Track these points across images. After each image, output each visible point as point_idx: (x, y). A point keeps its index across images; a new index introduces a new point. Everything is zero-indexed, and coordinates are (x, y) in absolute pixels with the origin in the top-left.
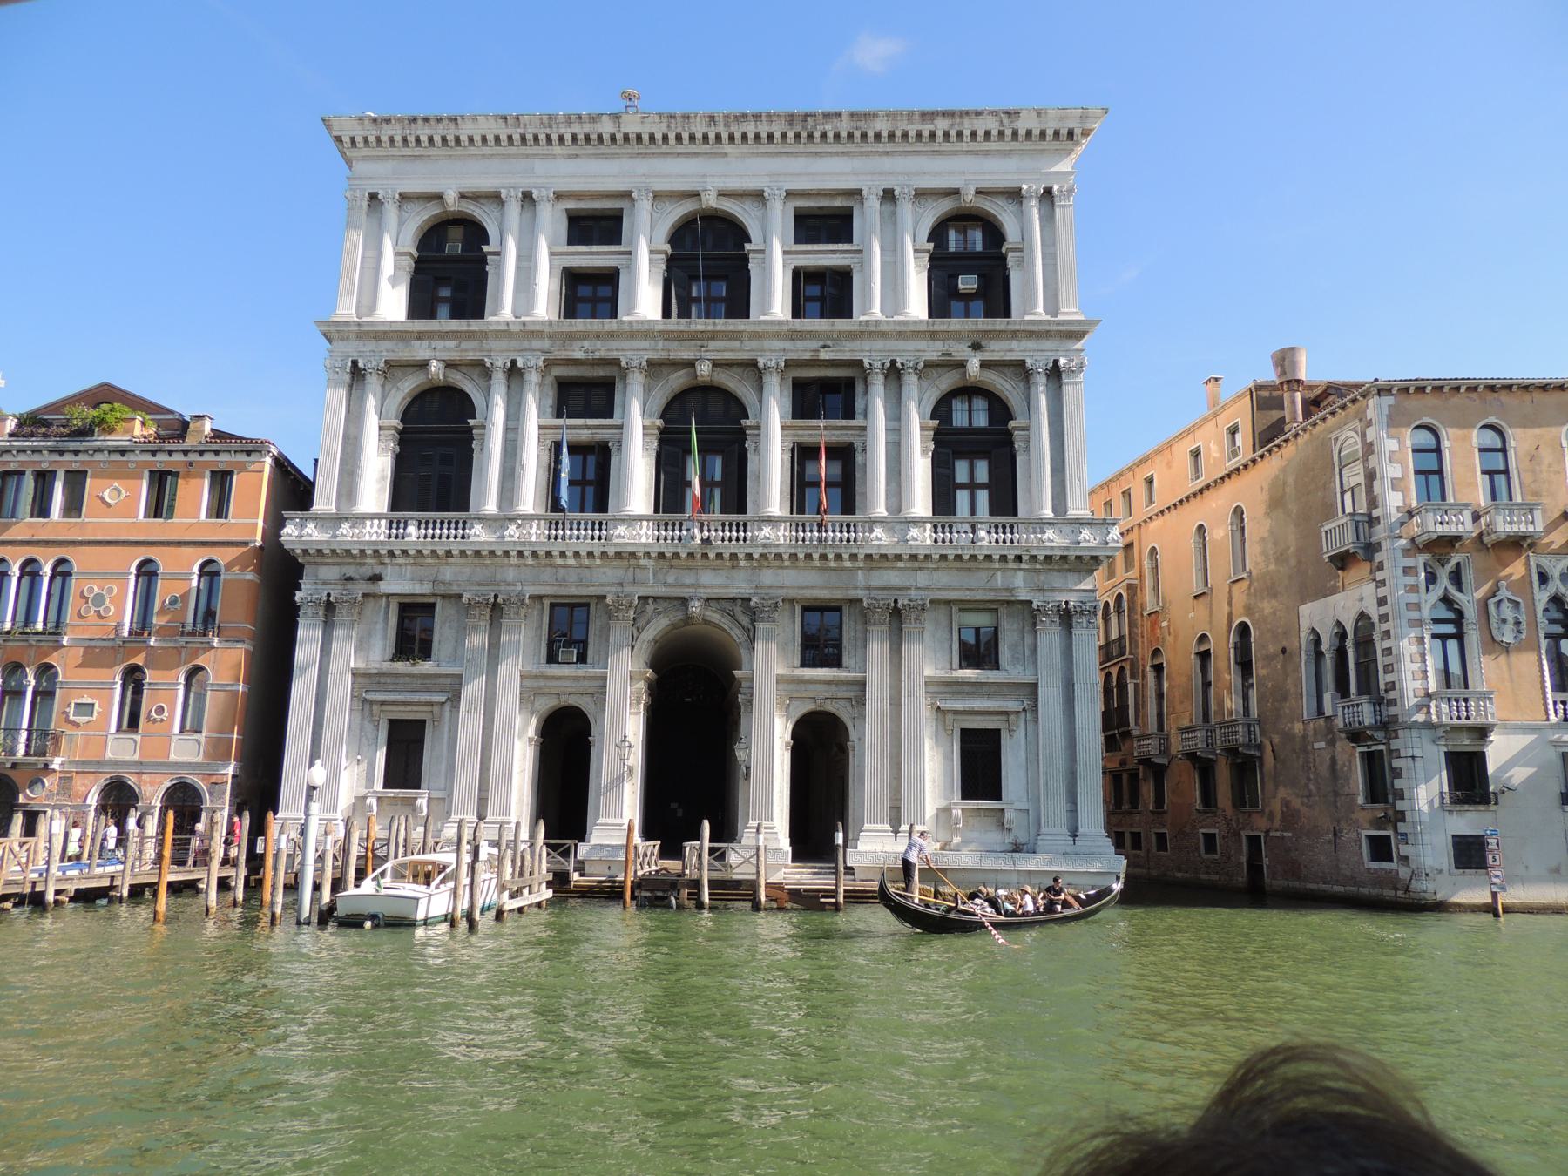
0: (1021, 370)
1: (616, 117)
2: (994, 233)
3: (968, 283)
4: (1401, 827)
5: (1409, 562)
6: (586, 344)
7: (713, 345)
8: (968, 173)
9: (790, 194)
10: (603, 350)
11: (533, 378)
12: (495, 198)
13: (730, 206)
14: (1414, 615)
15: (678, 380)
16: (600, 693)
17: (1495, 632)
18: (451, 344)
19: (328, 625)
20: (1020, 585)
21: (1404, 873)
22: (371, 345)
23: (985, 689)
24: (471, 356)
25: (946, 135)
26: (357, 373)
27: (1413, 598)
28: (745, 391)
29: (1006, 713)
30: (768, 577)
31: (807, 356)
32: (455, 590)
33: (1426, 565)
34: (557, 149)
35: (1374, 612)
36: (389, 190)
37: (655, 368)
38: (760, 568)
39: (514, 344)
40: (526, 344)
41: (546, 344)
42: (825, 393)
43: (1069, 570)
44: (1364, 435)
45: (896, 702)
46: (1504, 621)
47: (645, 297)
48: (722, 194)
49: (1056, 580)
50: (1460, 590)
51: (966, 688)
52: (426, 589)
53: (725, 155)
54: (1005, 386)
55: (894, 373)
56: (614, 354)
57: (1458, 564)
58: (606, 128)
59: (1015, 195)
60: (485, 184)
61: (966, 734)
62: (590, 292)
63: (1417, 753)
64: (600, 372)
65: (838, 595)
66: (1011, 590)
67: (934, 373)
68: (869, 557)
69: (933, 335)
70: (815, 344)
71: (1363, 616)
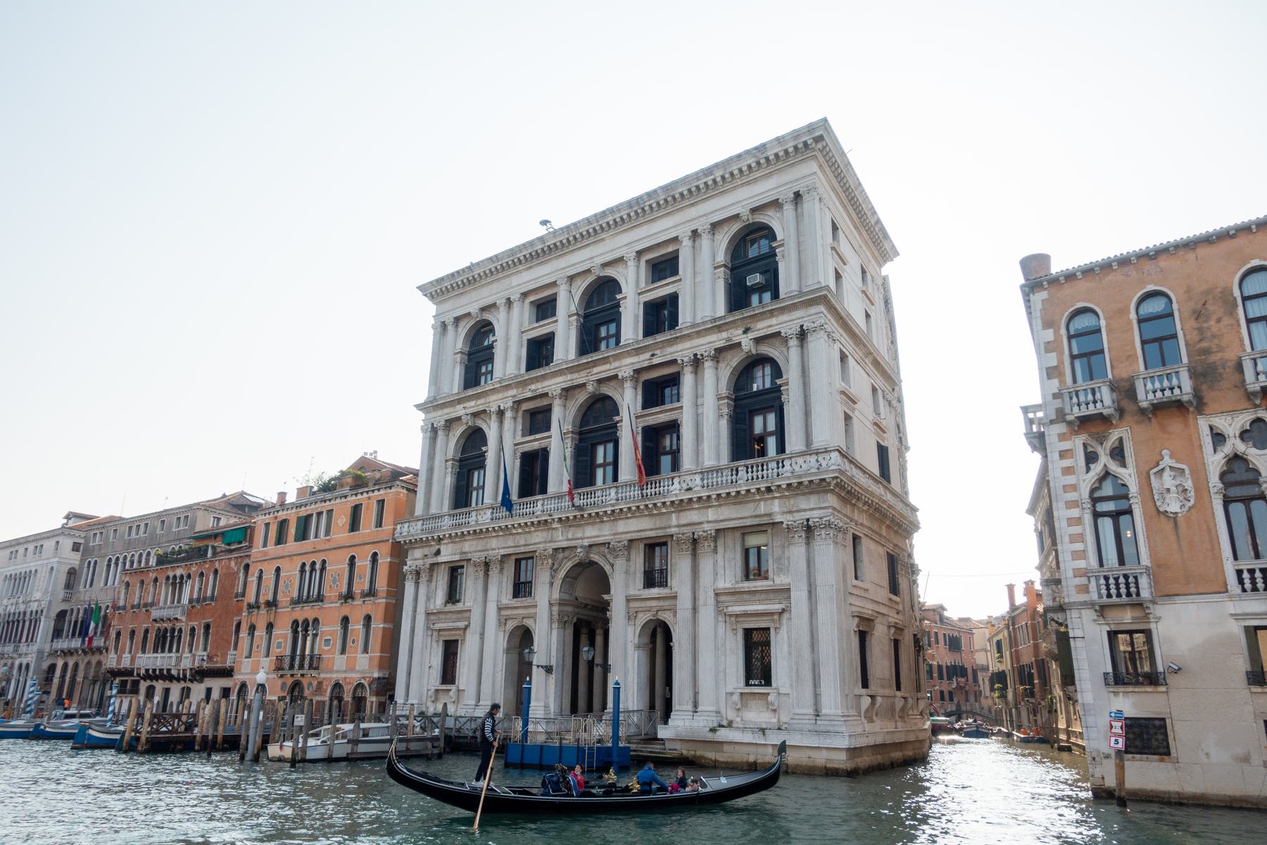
1: (541, 239)
2: (771, 235)
3: (755, 279)
5: (1066, 445)
6: (533, 387)
7: (596, 370)
10: (539, 387)
11: (509, 414)
12: (493, 306)
13: (610, 272)
14: (1072, 496)
15: (582, 397)
16: (533, 617)
17: (1158, 504)
18: (472, 403)
19: (417, 584)
20: (776, 508)
22: (440, 413)
23: (758, 596)
24: (481, 408)
25: (723, 178)
27: (1070, 480)
29: (772, 614)
30: (622, 526)
31: (646, 364)
32: (469, 556)
33: (1085, 446)
34: (521, 268)
37: (567, 392)
38: (616, 520)
39: (500, 396)
40: (506, 394)
41: (513, 392)
42: (659, 388)
43: (810, 493)
45: (695, 609)
46: (1168, 490)
47: (565, 347)
48: (605, 265)
49: (803, 502)
50: (1124, 465)
51: (746, 596)
52: (457, 558)
53: (603, 240)
55: (697, 362)
56: (546, 390)
57: (1121, 440)
58: (539, 247)
59: (776, 204)
61: (748, 633)
62: (539, 352)
63: (1078, 633)
64: (544, 402)
65: (661, 533)
66: (770, 515)
67: (729, 355)
68: (672, 502)
70: (647, 355)
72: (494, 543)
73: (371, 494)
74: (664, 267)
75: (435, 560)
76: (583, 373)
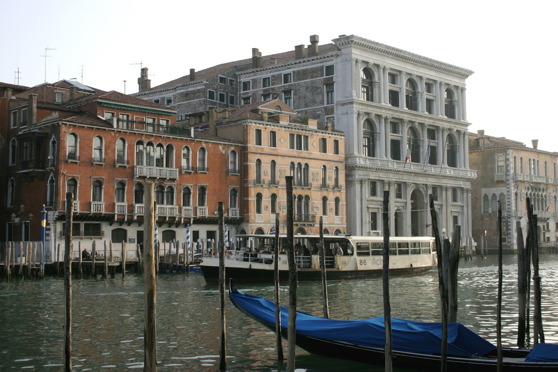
0: (459, 132)
4: (509, 236)
6: (398, 114)
7: (418, 118)
8: (453, 81)
9: (427, 79)
21: (509, 244)
26: (359, 115)
28: (420, 130)
35: (506, 193)
36: (360, 58)
44: (506, 157)
48: (417, 76)
54: (456, 135)
55: (443, 130)
56: (403, 118)
60: (378, 63)
69: (449, 122)
71: (502, 195)
72: (391, 176)
73: (330, 135)
74: (429, 87)
75: (368, 177)
76: (414, 117)
